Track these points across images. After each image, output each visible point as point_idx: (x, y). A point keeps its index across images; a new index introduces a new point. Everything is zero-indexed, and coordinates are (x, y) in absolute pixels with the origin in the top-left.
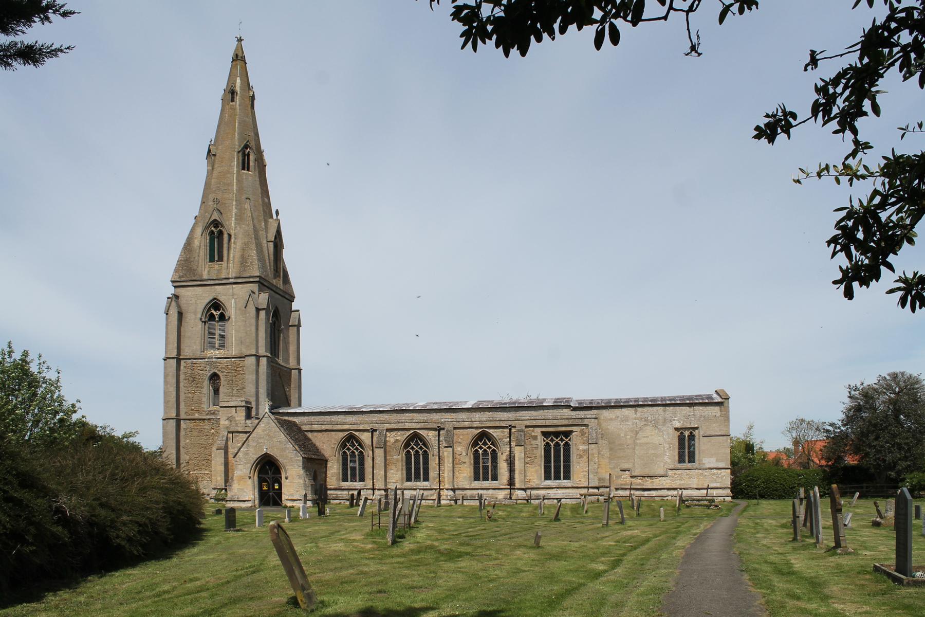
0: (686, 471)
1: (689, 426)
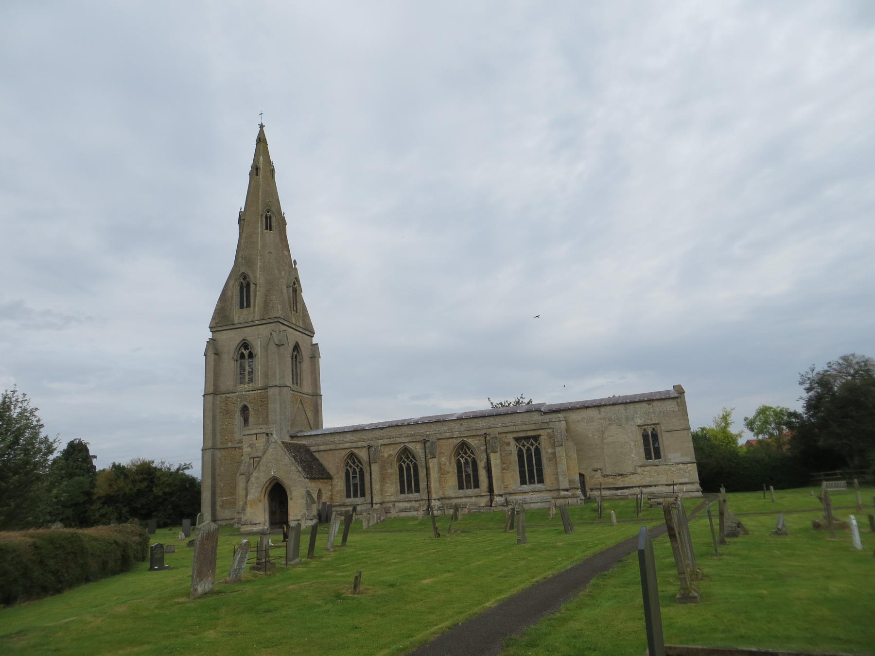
0: (654, 467)
1: (650, 422)
